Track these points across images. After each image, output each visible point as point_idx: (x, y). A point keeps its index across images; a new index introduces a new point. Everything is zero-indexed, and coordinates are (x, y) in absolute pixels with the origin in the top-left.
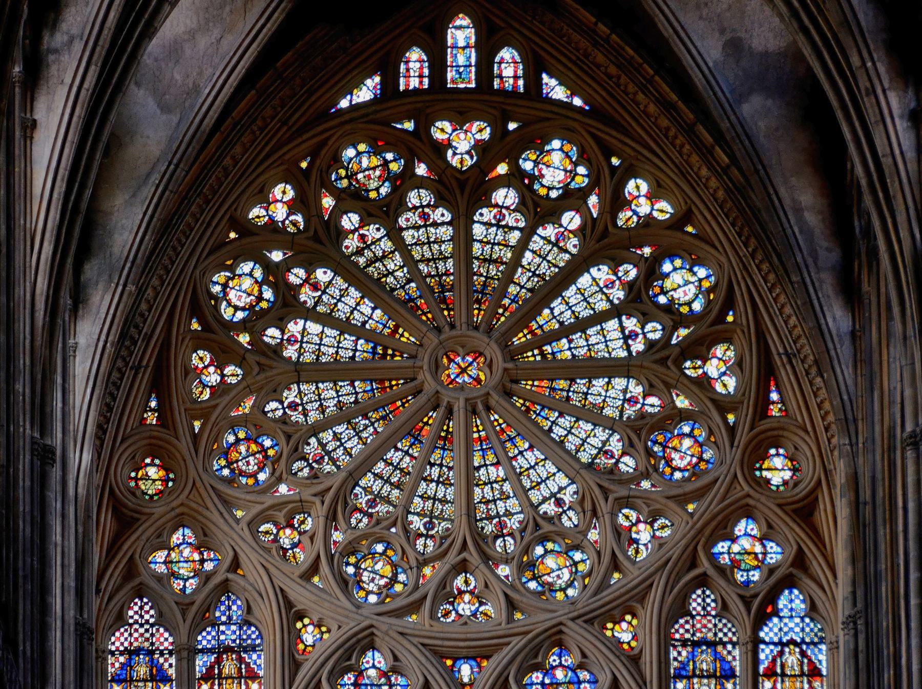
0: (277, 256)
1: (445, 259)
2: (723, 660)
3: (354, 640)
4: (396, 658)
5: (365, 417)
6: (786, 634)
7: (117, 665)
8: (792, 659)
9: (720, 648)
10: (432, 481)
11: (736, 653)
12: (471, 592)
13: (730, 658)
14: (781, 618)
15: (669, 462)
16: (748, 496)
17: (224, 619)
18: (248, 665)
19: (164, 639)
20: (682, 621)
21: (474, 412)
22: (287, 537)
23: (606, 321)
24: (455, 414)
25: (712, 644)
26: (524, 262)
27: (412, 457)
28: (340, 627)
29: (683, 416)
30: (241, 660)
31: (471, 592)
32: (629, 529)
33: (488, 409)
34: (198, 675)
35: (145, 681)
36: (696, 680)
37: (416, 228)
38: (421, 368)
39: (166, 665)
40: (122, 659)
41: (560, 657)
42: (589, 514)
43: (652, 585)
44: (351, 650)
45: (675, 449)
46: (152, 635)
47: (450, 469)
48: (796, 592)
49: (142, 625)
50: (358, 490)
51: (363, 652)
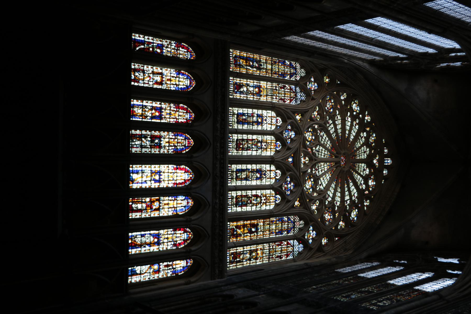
0: (361, 116)
1: (359, 157)
2: (291, 230)
3: (299, 129)
4: (295, 140)
5: (336, 135)
6: (295, 247)
7: (293, 64)
8: (290, 249)
9: (293, 229)
10: (325, 152)
11: (292, 234)
12: (305, 162)
13: (291, 232)
14: (298, 245)
15: (326, 213)
16: (323, 234)
17: (302, 95)
18: (293, 100)
19: (298, 78)
20: (298, 219)
21: (336, 164)
22: (316, 113)
23: (349, 197)
24: (336, 158)
25: (294, 227)
26: (358, 176)
27: (329, 147)
28: (301, 125)
29: (334, 216)
30: (294, 98)
31: (305, 162)
32: (315, 204)
33: (336, 168)
34: (291, 86)
35: (290, 71)
36: (287, 223)
37: (364, 150)
38: (345, 150)
39: (293, 78)
40: (294, 66)
41: (293, 186)
42: (319, 193)
43: (307, 210)
44: (296, 128)
45: (328, 214)
46: (299, 75)
47: (327, 156)
48: (303, 248)
49: (301, 72)
50: (323, 133)
51: (295, 132)
